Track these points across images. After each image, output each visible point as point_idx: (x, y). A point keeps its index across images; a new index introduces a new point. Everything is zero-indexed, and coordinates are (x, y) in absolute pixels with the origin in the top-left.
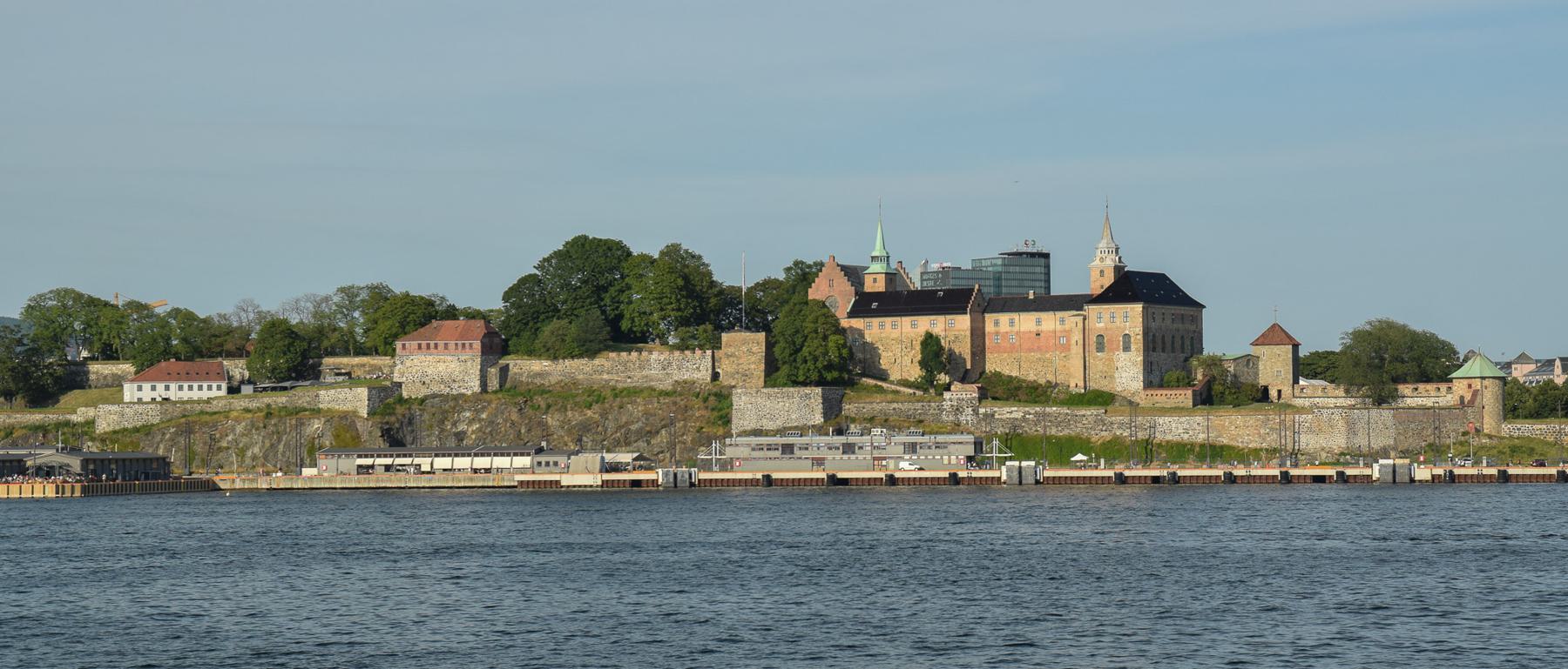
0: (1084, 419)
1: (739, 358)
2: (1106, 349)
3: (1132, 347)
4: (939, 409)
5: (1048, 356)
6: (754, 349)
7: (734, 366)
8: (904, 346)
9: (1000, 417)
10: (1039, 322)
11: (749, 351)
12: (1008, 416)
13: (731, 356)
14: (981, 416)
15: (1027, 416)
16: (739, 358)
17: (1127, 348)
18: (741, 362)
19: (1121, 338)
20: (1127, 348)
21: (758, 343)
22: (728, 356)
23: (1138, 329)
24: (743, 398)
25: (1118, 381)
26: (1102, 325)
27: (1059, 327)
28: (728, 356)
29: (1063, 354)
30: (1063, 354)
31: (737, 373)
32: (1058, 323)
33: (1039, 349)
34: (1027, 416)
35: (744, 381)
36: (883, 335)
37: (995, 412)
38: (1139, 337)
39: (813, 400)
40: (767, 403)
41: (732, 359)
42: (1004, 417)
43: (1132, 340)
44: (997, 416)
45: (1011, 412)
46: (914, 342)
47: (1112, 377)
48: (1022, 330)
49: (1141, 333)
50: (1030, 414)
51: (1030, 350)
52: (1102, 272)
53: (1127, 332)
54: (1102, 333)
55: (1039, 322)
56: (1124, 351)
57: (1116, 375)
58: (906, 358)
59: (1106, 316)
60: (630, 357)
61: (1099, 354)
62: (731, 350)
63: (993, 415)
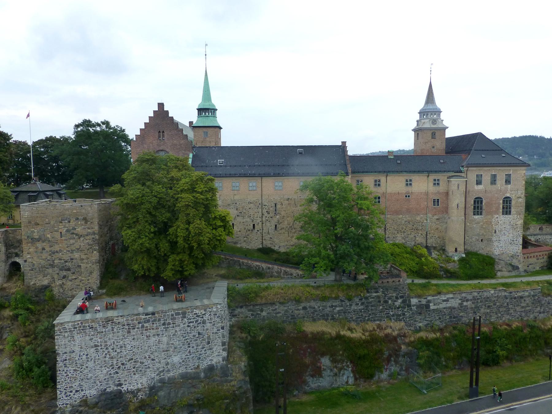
0: (523, 300)
2: (484, 212)
4: (362, 304)
5: (418, 218)
6: (79, 230)
7: (45, 255)
8: (265, 211)
9: (435, 307)
10: (409, 183)
11: (71, 232)
12: (444, 305)
13: (38, 240)
14: (414, 308)
15: (465, 304)
16: (51, 243)
17: (507, 210)
18: (56, 248)
19: (501, 202)
20: (507, 210)
21: (85, 220)
22: (33, 241)
23: (519, 193)
24: (78, 338)
25: (496, 244)
26: (480, 187)
27: (432, 189)
28: (33, 241)
29: (436, 217)
30: (436, 217)
31: (52, 266)
32: (431, 184)
33: (409, 211)
34: (465, 304)
35: (64, 277)
36: (236, 197)
37: (429, 301)
38: (520, 200)
39: (208, 325)
40: (127, 341)
41: (40, 245)
42: (441, 306)
43: (513, 203)
44: (432, 307)
45: (447, 301)
46: (278, 206)
47: (490, 240)
48: (389, 190)
49: (523, 196)
50: (467, 301)
51: (397, 212)
53: (508, 195)
54: (480, 196)
55: (409, 183)
56: (503, 214)
57: (494, 239)
58: (268, 224)
59: (487, 179)
61: (476, 217)
63: (427, 306)
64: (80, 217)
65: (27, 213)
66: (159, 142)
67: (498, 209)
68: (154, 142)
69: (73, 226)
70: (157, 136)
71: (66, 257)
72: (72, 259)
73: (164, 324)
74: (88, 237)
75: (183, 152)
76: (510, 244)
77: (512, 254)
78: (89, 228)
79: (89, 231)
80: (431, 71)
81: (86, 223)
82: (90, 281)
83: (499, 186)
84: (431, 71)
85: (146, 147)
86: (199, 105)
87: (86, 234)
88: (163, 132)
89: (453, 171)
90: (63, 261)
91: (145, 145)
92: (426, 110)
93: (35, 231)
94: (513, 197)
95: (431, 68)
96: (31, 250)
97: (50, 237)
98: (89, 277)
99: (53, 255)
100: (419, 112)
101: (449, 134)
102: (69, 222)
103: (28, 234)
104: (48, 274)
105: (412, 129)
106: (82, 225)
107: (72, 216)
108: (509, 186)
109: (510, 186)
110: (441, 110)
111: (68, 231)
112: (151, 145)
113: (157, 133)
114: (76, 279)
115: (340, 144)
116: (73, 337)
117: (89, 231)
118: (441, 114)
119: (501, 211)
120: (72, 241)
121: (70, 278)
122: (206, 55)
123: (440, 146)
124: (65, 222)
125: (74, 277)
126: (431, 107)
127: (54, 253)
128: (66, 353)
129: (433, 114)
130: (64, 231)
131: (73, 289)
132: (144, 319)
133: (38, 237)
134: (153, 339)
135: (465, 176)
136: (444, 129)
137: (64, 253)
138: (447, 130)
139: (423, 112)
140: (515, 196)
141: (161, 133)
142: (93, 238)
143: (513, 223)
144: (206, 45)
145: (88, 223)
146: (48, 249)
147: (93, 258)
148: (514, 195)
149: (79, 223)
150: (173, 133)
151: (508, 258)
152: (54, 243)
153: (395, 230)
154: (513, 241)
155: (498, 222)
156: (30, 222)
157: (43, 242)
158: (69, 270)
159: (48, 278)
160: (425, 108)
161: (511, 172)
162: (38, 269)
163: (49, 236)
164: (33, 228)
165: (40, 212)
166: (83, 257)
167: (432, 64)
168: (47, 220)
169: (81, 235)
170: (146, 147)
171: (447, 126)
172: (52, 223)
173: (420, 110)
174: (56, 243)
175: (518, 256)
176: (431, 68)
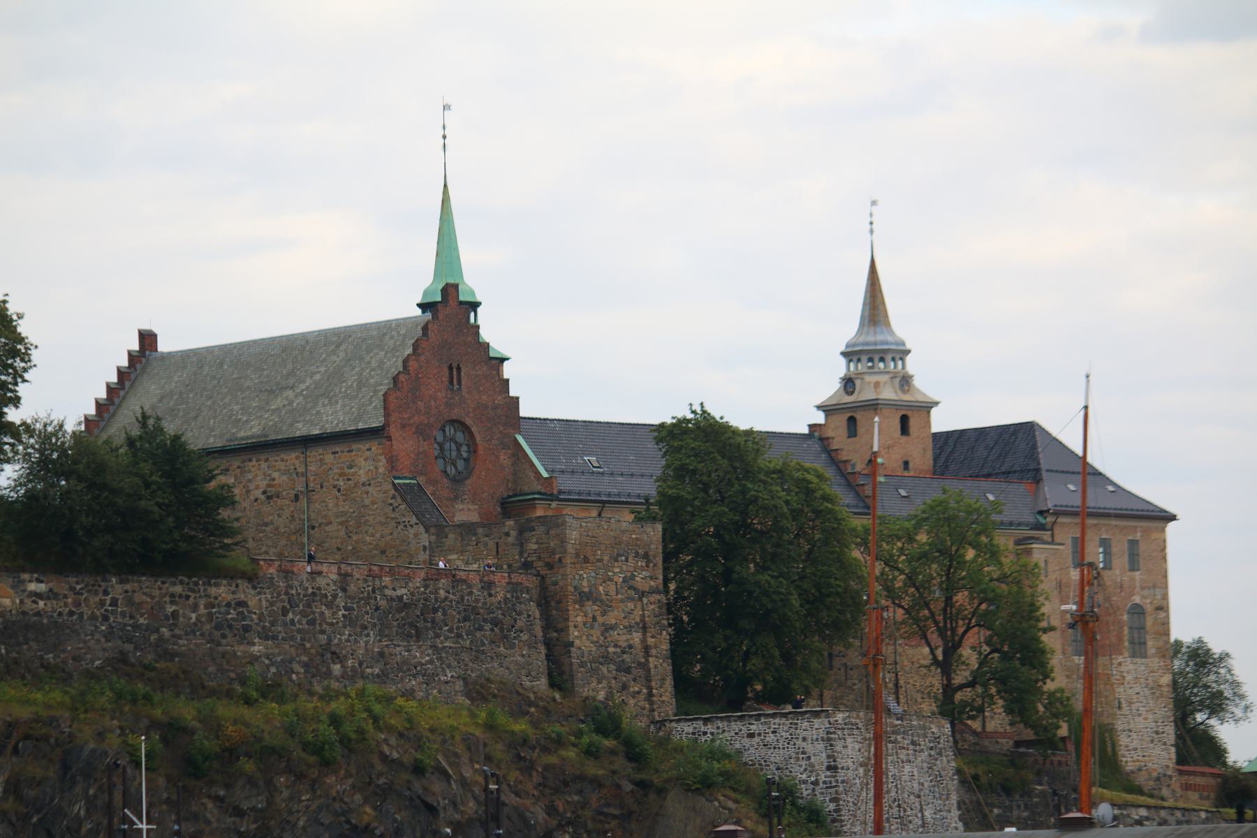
1: (606, 607)
3: (1150, 643)
6: (641, 580)
18: (611, 619)
19: (1125, 617)
21: (646, 556)
22: (585, 597)
24: (849, 740)
28: (585, 597)
31: (606, 659)
41: (590, 608)
52: (904, 420)
53: (1137, 599)
57: (1120, 725)
60: (321, 582)
62: (585, 578)
64: (640, 551)
65: (574, 533)
66: (449, 396)
67: (1120, 640)
68: (439, 394)
69: (632, 569)
70: (446, 379)
71: (622, 638)
72: (630, 647)
73: (913, 743)
74: (652, 599)
75: (501, 428)
76: (1152, 741)
77: (1160, 770)
78: (651, 578)
79: (652, 583)
80: (871, 223)
81: (647, 566)
82: (664, 698)
83: (1117, 572)
84: (871, 223)
85: (422, 408)
86: (426, 293)
87: (647, 590)
88: (459, 369)
89: (1027, 525)
90: (619, 650)
91: (419, 403)
92: (876, 344)
93: (585, 576)
94: (1149, 608)
95: (871, 215)
96: (579, 619)
97: (602, 592)
98: (662, 690)
99: (607, 634)
100: (843, 348)
101: (941, 421)
102: (627, 560)
103: (576, 583)
104: (604, 677)
105: (819, 401)
106: (642, 569)
107: (630, 548)
108: (1137, 573)
109: (1141, 574)
110: (908, 346)
111: (625, 580)
112: (433, 403)
113: (446, 370)
114: (638, 693)
115: (806, 431)
116: (845, 739)
117: (652, 583)
118: (909, 359)
119: (1126, 644)
120: (631, 605)
121: (631, 689)
122: (444, 137)
123: (922, 458)
124: (622, 561)
125: (637, 689)
126: (879, 338)
127: (607, 630)
128: (843, 768)
129: (855, 358)
130: (621, 579)
131: (637, 715)
132: (896, 726)
133: (586, 590)
134: (907, 768)
135: (1050, 540)
136: (926, 408)
137: (621, 632)
138: (934, 411)
139: (861, 352)
140: (1151, 603)
141: (454, 370)
142: (659, 601)
143: (1154, 682)
144: (446, 107)
145: (651, 565)
146: (600, 619)
147: (663, 647)
148: (1148, 601)
149: (640, 564)
150: (480, 372)
151: (1151, 783)
152: (607, 606)
153: (918, 691)
154: (1157, 733)
155: (1124, 677)
156: (577, 555)
157: (594, 603)
158: (628, 670)
159: (605, 688)
160: (862, 339)
161: (1138, 536)
162: (589, 665)
163: (601, 588)
164: (582, 568)
165: (590, 534)
166: (650, 641)
167: (874, 203)
168: (599, 552)
169: (643, 592)
170: (423, 411)
171: (936, 399)
172: (606, 558)
173: (847, 346)
174: (611, 607)
175: (1170, 777)
176: (871, 215)
